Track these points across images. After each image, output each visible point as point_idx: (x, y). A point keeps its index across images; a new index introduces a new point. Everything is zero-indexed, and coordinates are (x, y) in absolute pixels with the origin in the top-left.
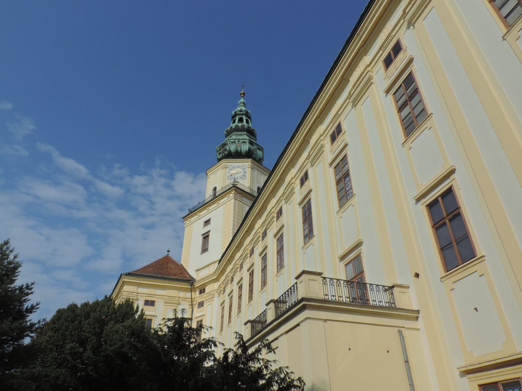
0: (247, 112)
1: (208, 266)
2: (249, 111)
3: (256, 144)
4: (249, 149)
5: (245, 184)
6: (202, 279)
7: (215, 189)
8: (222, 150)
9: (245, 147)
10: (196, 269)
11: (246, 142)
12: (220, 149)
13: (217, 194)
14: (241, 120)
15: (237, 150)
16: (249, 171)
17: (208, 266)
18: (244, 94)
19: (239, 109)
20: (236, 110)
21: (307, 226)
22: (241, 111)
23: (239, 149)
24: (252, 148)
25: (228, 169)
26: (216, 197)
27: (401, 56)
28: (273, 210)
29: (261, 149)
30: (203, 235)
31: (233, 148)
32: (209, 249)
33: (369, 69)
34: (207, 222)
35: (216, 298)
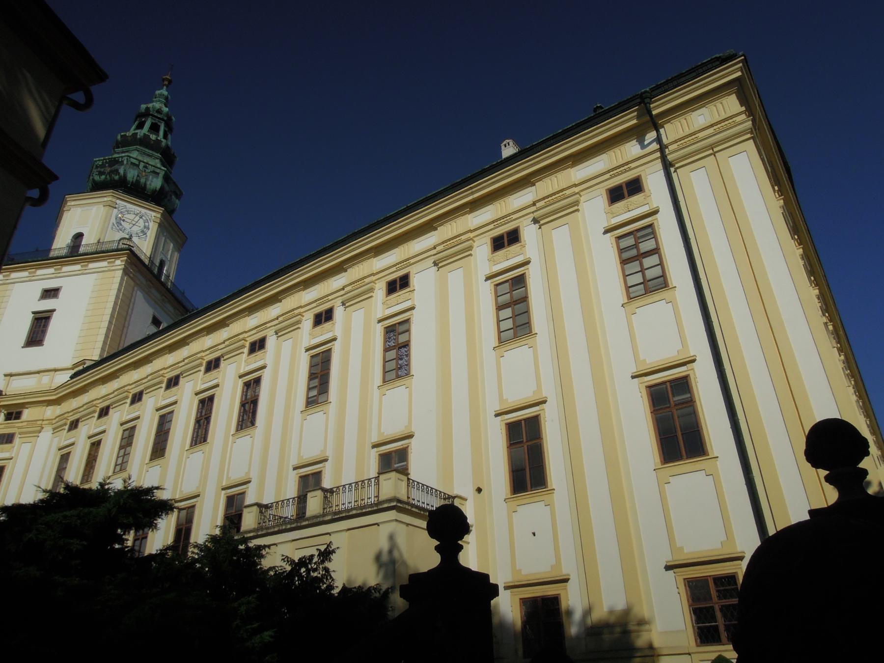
0: (170, 119)
1: (38, 372)
2: (174, 118)
3: (174, 183)
4: (162, 188)
5: (145, 247)
6: (15, 395)
7: (79, 236)
8: (108, 170)
9: (156, 183)
10: (8, 372)
11: (158, 174)
12: (103, 166)
13: (82, 250)
14: (155, 128)
15: (138, 182)
16: (153, 228)
17: (38, 372)
18: (170, 82)
19: (157, 105)
20: (150, 105)
21: (315, 382)
22: (159, 111)
23: (143, 180)
24: (167, 188)
25: (115, 211)
26: (75, 251)
27: (514, 248)
28: (245, 335)
29: (179, 195)
30: (34, 313)
31: (132, 175)
32: (45, 342)
33: (471, 235)
34: (51, 293)
35: (46, 435)
